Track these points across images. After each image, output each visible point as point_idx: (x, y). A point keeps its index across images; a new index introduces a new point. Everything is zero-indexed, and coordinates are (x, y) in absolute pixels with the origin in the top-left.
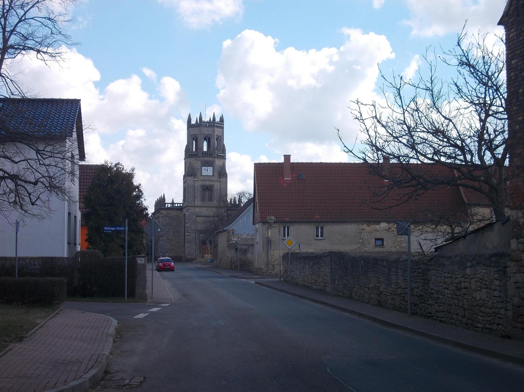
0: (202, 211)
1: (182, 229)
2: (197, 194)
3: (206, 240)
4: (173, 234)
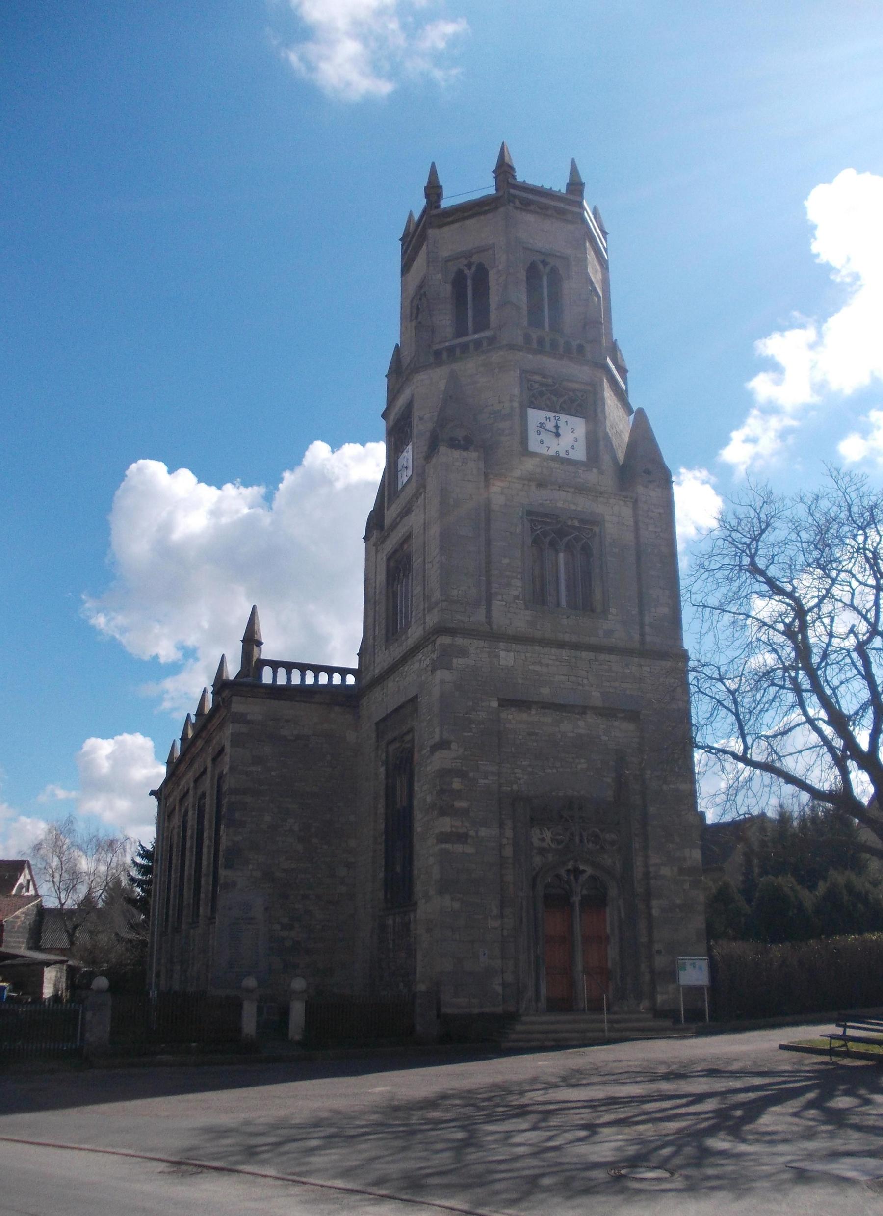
0: (537, 668)
2: (506, 561)
3: (568, 871)
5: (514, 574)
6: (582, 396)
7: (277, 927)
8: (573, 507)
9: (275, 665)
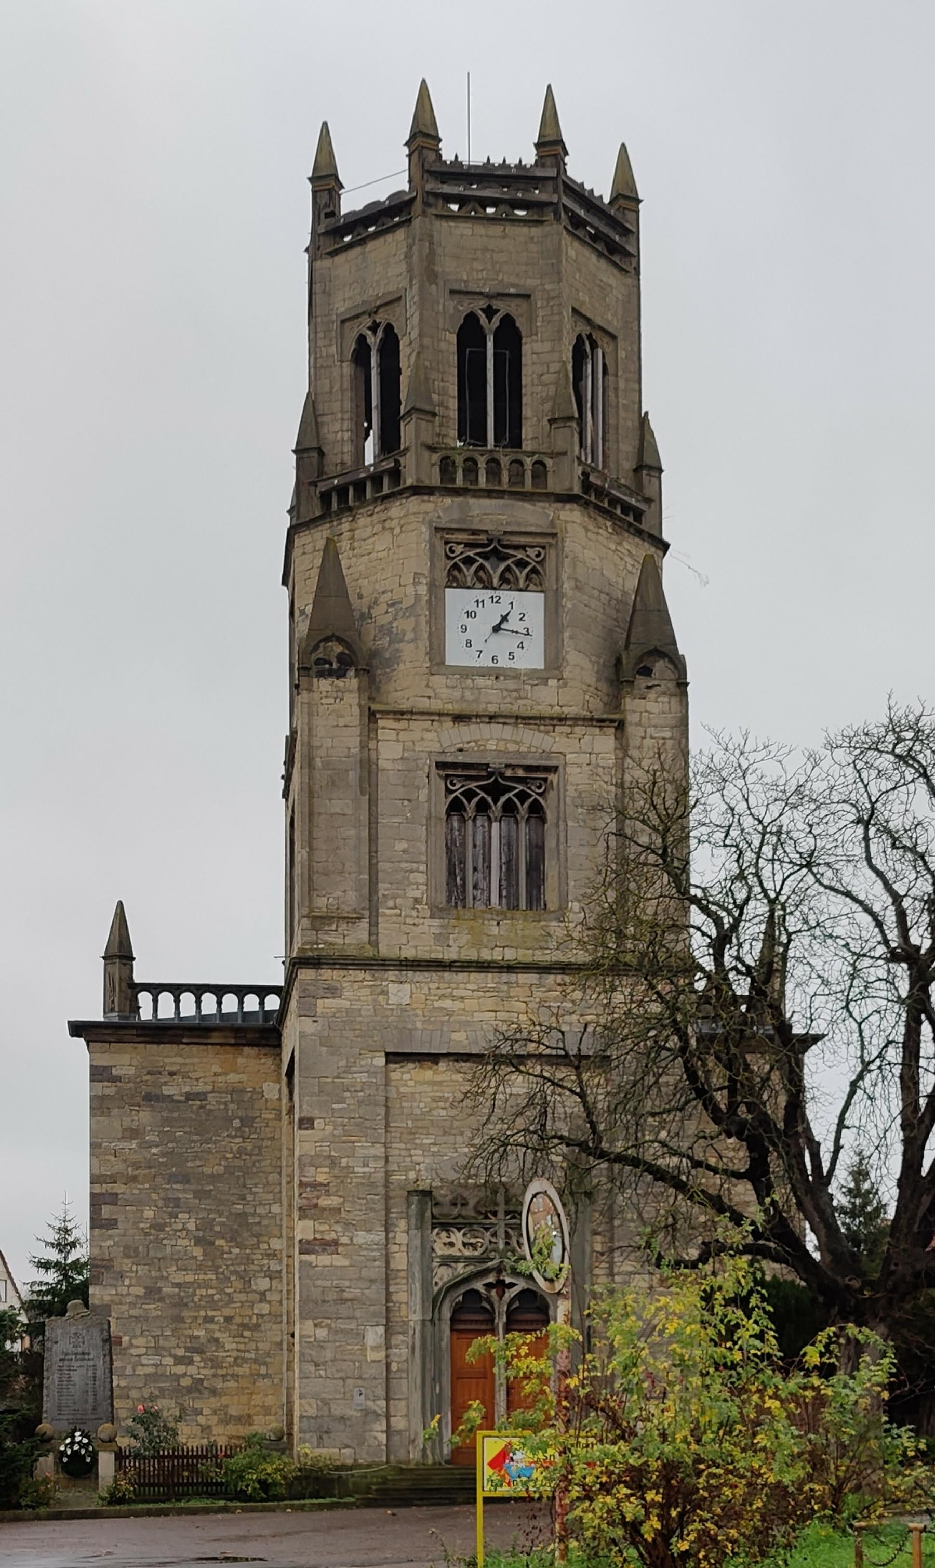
0: (447, 1004)
1: (275, 1209)
2: (401, 846)
3: (489, 1286)
4: (198, 1252)
5: (415, 866)
6: (538, 555)
7: (169, 1361)
8: (512, 747)
9: (156, 989)
